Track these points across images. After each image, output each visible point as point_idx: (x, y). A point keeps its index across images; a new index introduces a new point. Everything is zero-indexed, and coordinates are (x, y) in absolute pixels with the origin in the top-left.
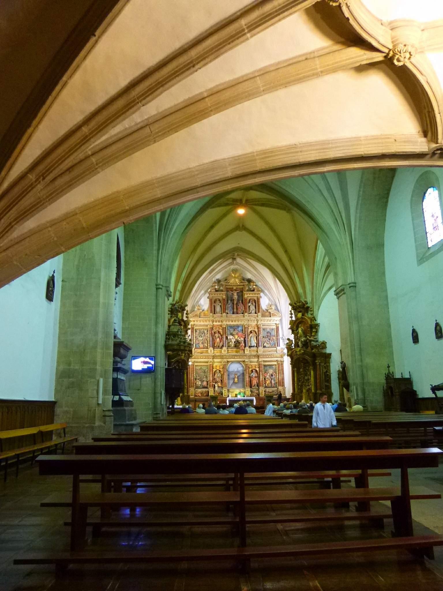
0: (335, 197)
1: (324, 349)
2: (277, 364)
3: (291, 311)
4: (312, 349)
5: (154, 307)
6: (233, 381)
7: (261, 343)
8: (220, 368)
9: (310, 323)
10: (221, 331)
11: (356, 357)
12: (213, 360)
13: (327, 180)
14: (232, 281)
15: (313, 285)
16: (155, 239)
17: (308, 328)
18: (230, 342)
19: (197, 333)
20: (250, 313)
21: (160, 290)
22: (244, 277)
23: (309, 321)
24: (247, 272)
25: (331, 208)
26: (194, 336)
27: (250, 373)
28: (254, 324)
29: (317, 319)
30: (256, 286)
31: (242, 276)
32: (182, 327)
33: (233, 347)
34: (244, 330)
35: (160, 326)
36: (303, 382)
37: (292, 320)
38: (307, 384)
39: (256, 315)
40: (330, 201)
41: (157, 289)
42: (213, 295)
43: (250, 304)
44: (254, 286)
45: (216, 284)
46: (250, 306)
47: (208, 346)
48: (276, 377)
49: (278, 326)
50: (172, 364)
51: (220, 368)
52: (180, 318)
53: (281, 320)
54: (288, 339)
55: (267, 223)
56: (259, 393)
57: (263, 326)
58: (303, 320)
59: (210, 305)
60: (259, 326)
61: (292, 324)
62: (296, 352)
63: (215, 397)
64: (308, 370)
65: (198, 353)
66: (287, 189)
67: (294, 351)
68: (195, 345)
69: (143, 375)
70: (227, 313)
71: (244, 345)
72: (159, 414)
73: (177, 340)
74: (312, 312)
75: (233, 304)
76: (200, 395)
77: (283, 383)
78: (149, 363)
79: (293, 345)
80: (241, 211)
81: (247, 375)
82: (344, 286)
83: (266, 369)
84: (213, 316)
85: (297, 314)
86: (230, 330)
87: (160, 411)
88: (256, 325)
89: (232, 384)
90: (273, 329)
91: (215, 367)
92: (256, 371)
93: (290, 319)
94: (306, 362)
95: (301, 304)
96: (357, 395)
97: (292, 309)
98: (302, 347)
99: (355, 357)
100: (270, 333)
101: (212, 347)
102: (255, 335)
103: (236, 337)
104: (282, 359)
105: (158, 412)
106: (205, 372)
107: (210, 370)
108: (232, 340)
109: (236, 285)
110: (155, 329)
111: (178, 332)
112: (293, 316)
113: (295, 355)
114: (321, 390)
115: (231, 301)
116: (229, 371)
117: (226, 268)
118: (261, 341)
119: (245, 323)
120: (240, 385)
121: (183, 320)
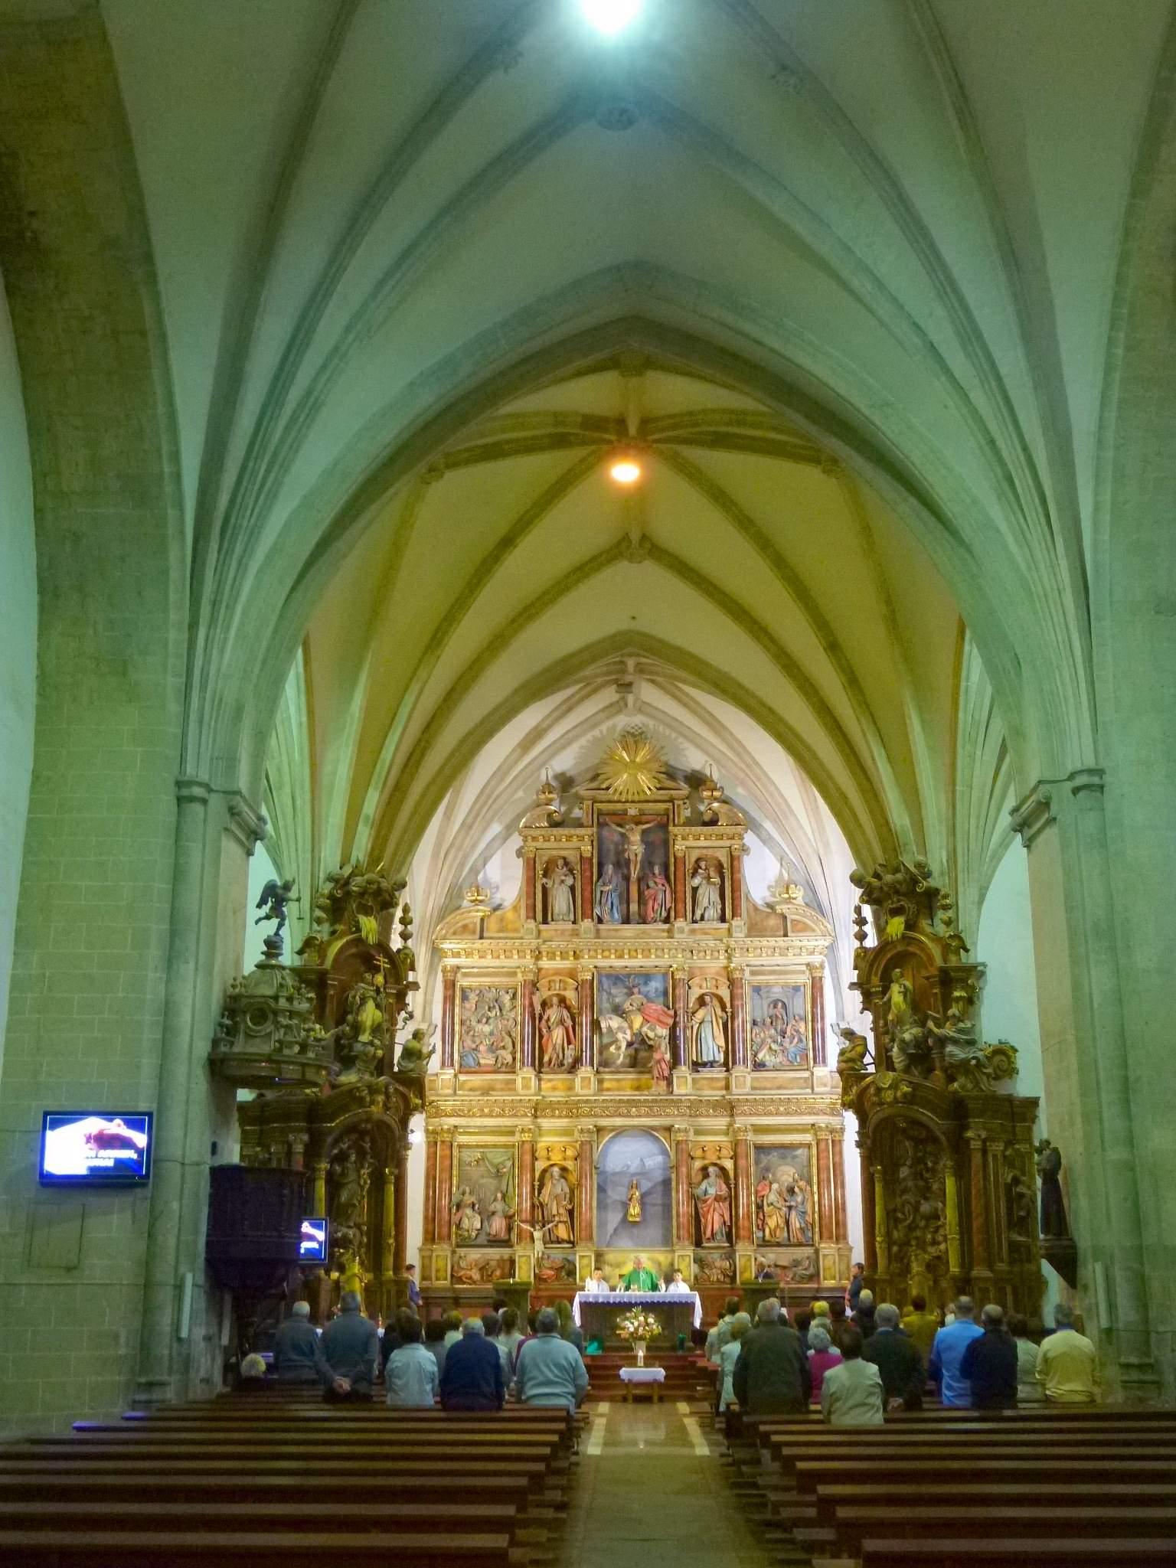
0: (999, 379)
1: (1007, 1080)
3: (858, 910)
4: (951, 1079)
5: (162, 886)
7: (745, 1050)
9: (939, 962)
10: (571, 995)
11: (1106, 1125)
12: (534, 1123)
13: (962, 300)
14: (622, 781)
15: (954, 792)
16: (174, 574)
17: (932, 986)
18: (611, 1044)
19: (467, 1005)
20: (698, 916)
21: (197, 808)
22: (672, 763)
23: (936, 951)
24: (686, 744)
25: (986, 431)
26: (457, 1020)
27: (695, 1180)
28: (714, 965)
29: (975, 944)
30: (725, 801)
31: (663, 758)
32: (380, 979)
33: (623, 1065)
34: (671, 990)
35: (187, 969)
36: (911, 1228)
37: (865, 950)
38: (929, 1236)
39: (726, 925)
40: (978, 398)
41: (180, 800)
42: (540, 844)
43: (696, 881)
44: (716, 805)
46: (700, 891)
47: (514, 1059)
48: (809, 1200)
49: (817, 974)
50: (330, 1140)
51: (565, 1159)
52: (372, 939)
53: (832, 949)
54: (849, 1034)
55: (745, 523)
57: (753, 973)
58: (911, 949)
59: (528, 884)
60: (737, 975)
61: (863, 965)
62: (879, 1090)
63: (516, 1291)
64: (933, 1171)
65: (471, 1090)
66: (788, 353)
67: (868, 1086)
68: (461, 1057)
69: (94, 1200)
70: (600, 921)
71: (668, 1057)
72: (162, 1384)
73: (270, 1034)
74: (950, 913)
75: (627, 878)
76: (476, 1276)
77: (841, 1225)
78: (126, 1144)
79: (868, 1059)
80: (625, 472)
81: (683, 1188)
82: (1048, 786)
83: (765, 1160)
84: (539, 932)
85: (887, 923)
86: (610, 994)
87: (170, 1372)
88: (725, 974)
90: (796, 989)
92: (723, 1170)
93: (857, 944)
94: (925, 1138)
95: (899, 876)
96: (1112, 1307)
97: (863, 901)
98: (907, 1070)
99: (1101, 1120)
100: (784, 1006)
101: (533, 1064)
103: (637, 1021)
104: (834, 1121)
105: (158, 1378)
106: (498, 1175)
107: (521, 1167)
108: (620, 1036)
109: (636, 798)
110: (163, 987)
111: (276, 998)
112: (869, 929)
113: (874, 1104)
114: (991, 1267)
115: (618, 865)
117: (594, 726)
118: (744, 1041)
119: (676, 961)
120: (654, 1231)
121: (383, 947)
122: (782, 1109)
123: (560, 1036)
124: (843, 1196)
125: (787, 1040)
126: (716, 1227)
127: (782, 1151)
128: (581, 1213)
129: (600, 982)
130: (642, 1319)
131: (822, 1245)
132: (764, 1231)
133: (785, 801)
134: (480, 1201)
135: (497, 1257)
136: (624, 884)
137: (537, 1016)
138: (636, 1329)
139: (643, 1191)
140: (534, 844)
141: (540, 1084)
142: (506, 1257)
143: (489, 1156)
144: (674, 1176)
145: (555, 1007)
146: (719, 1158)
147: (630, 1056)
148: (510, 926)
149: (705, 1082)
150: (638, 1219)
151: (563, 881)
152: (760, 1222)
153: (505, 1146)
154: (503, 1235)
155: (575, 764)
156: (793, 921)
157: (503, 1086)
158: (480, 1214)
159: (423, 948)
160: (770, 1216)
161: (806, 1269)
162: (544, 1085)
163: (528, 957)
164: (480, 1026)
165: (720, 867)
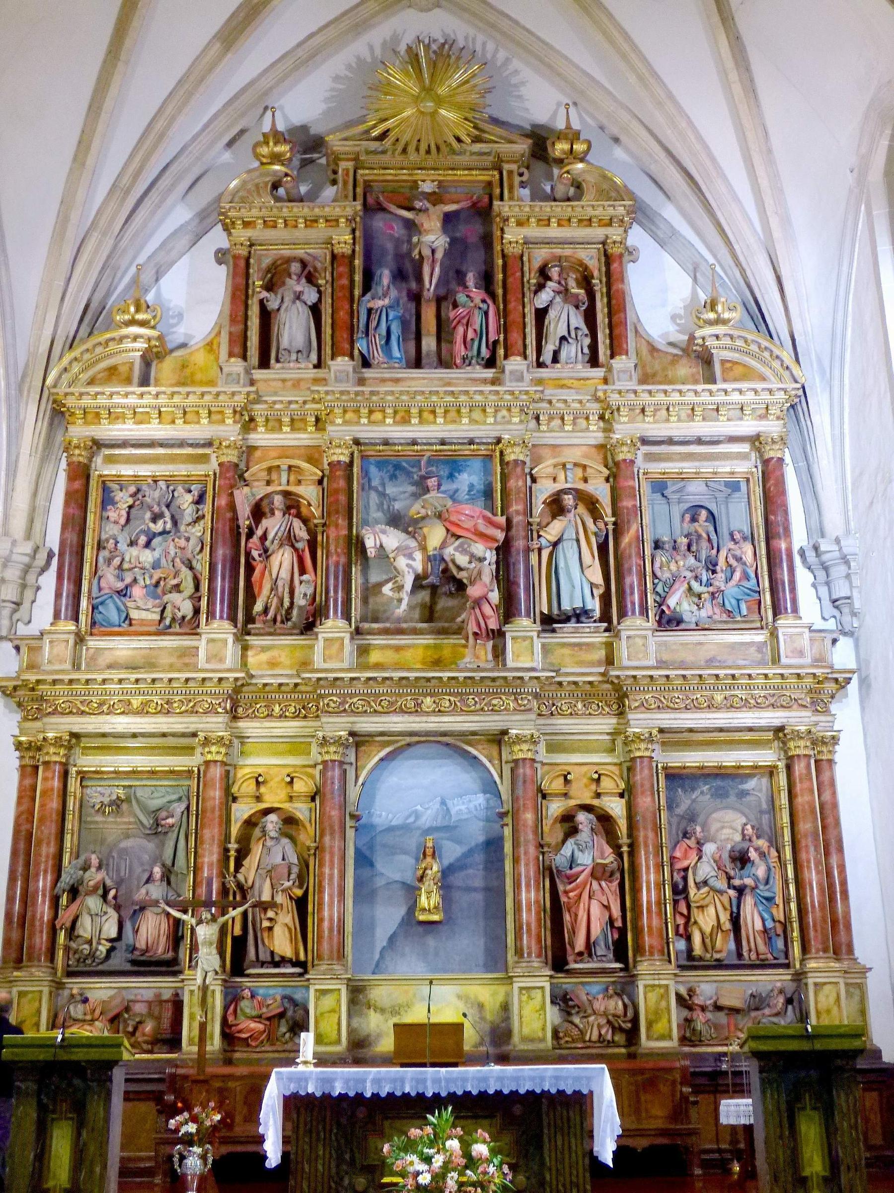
2: (781, 765)
6: (402, 911)
8: (291, 798)
10: (309, 492)
12: (228, 727)
18: (381, 585)
19: (112, 514)
20: (547, 357)
39: (599, 373)
42: (258, 233)
44: (580, 166)
45: (283, 148)
46: (552, 314)
47: (197, 611)
51: (291, 798)
56: (635, 1020)
57: (649, 457)
59: (234, 297)
60: (623, 455)
63: (76, 1068)
71: (495, 596)
75: (416, 298)
86: (383, 495)
88: (600, 458)
89: (392, 939)
90: (734, 487)
91: (249, 787)
92: (605, 820)
101: (233, 619)
102: (589, 522)
103: (435, 535)
108: (402, 562)
115: (399, 275)
116: (371, 827)
122: (719, 697)
123: (286, 565)
124: (842, 868)
125: (720, 576)
126: (596, 931)
127: (719, 783)
128: (321, 904)
129: (365, 473)
130: (454, 1144)
131: (812, 964)
132: (689, 938)
133: (706, 147)
134: (119, 884)
135: (149, 995)
136: (412, 306)
137: (244, 531)
138: (439, 1177)
139: (446, 862)
140: (249, 233)
141: (244, 656)
142: (167, 995)
143: (140, 793)
144: (507, 832)
145: (278, 514)
146: (598, 795)
147: (423, 606)
148: (199, 376)
149: (566, 651)
150: (436, 918)
151: (298, 297)
152: (681, 921)
153: (172, 773)
154: (161, 950)
155: (327, 113)
156: (723, 362)
157: (173, 660)
158: (117, 908)
159: (32, 409)
160: (701, 908)
161: (777, 1014)
162: (253, 659)
163: (229, 421)
164: (134, 551)
165: (586, 281)
